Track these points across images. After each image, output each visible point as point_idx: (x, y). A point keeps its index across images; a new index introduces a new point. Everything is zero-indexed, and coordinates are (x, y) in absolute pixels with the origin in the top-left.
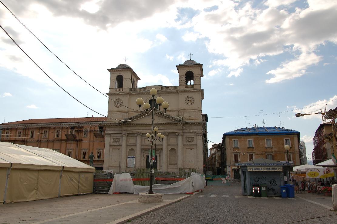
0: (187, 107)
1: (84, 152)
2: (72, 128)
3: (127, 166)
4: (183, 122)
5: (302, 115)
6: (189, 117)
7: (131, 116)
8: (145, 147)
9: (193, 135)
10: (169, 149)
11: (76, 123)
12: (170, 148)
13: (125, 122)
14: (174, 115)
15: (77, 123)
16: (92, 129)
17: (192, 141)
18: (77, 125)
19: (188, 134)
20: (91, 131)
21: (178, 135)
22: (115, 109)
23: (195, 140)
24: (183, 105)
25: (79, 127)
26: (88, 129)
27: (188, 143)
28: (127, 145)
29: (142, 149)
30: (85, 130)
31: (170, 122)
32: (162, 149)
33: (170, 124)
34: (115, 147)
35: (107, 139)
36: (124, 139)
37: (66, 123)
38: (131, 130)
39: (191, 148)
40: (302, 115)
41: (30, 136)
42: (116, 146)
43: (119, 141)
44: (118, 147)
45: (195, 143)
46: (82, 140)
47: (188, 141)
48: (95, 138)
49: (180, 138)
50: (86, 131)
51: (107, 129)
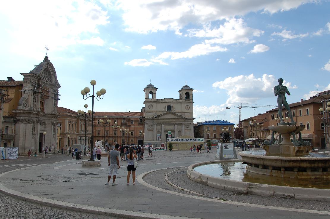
0: (186, 111)
2: (124, 119)
5: (229, 108)
6: (187, 115)
7: (159, 114)
8: (165, 130)
9: (189, 124)
10: (178, 131)
12: (178, 130)
13: (156, 117)
14: (180, 114)
16: (136, 120)
17: (189, 127)
19: (187, 124)
20: (135, 121)
21: (182, 125)
23: (190, 126)
24: (184, 110)
25: (127, 119)
27: (187, 128)
28: (157, 129)
29: (164, 131)
31: (179, 118)
32: (175, 131)
33: (179, 119)
34: (150, 130)
35: (146, 125)
36: (155, 125)
38: (159, 121)
40: (229, 108)
41: (98, 123)
42: (151, 130)
43: (152, 127)
44: (152, 130)
45: (190, 128)
46: (130, 126)
48: (138, 125)
49: (183, 126)
51: (146, 120)
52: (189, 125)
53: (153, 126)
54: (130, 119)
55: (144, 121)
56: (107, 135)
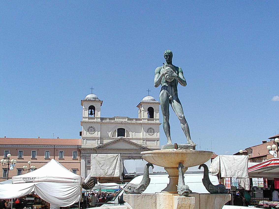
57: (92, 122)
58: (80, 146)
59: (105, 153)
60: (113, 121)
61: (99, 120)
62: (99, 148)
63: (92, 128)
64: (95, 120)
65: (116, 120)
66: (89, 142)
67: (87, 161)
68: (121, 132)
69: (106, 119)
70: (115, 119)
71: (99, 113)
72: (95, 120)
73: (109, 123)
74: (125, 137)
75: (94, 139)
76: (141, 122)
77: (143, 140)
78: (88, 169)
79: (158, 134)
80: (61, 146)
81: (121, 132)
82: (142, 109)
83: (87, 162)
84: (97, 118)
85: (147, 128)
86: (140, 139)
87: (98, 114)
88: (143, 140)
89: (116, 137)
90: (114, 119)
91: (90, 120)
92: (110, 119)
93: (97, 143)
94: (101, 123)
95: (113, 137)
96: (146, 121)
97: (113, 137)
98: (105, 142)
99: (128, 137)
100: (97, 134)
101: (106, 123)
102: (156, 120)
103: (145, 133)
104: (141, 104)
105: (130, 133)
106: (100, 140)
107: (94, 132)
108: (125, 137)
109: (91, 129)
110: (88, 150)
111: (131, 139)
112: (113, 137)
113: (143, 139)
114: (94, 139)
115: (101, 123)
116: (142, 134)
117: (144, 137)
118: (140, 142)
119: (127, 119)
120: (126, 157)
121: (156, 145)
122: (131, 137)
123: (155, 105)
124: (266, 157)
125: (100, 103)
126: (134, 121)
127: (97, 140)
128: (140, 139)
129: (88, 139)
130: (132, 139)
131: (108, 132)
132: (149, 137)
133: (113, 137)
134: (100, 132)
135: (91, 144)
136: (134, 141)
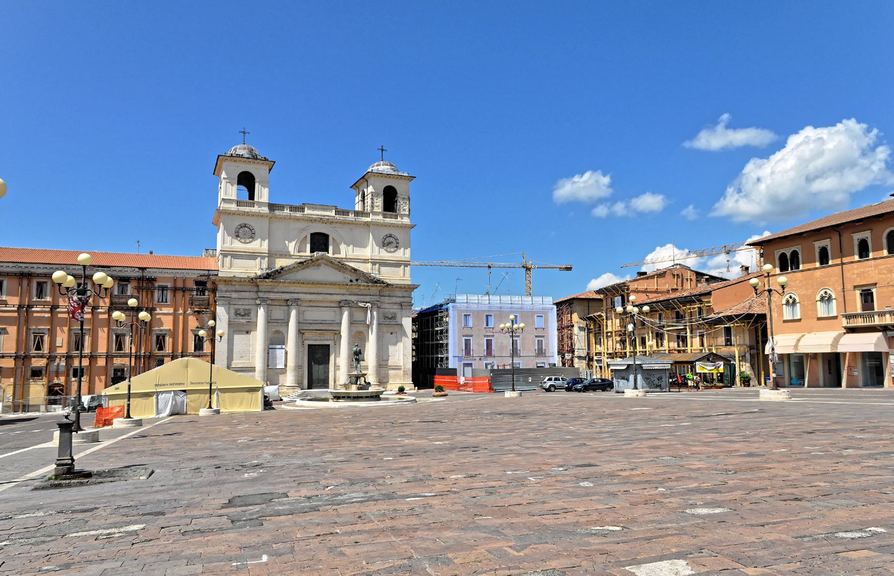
1: (158, 337)
3: (268, 366)
4: (384, 283)
9: (396, 307)
10: (353, 333)
11: (137, 270)
15: (140, 268)
16: (180, 284)
17: (394, 317)
18: (139, 274)
22: (238, 245)
23: (398, 316)
25: (140, 279)
26: (169, 285)
30: (159, 287)
37: (109, 267)
39: (392, 331)
47: (386, 317)
50: (163, 289)
52: (395, 309)
53: (253, 314)
54: (152, 280)
55: (214, 291)
56: (38, 348)
57: (247, 214)
58: (216, 273)
59: (280, 290)
60: (299, 214)
61: (265, 210)
62: (265, 278)
63: (246, 229)
64: (256, 209)
65: (307, 211)
66: (237, 262)
67: (233, 311)
68: (320, 242)
69: (281, 207)
70: (306, 209)
71: (266, 191)
72: (256, 209)
73: (290, 218)
74: (330, 254)
75: (252, 256)
76: (369, 219)
77: (371, 262)
78: (240, 332)
79: (408, 251)
80: (161, 270)
81: (320, 242)
82: (370, 189)
83: (233, 315)
84: (261, 204)
85: (383, 235)
86: (365, 261)
87: (263, 194)
88: (371, 262)
89: (308, 253)
90: (302, 209)
91: (242, 209)
92: (293, 208)
93: (258, 267)
94: (271, 219)
95: (301, 254)
96: (380, 218)
97: (298, 252)
98: (280, 263)
99: (336, 256)
100: (260, 245)
101: (284, 218)
102: (402, 216)
103: (377, 248)
104: (365, 177)
105: (343, 247)
106: (266, 259)
107: (251, 240)
108: (330, 254)
109: (244, 231)
110: (237, 284)
111: (342, 258)
112: (299, 252)
113: (371, 259)
114: (252, 256)
115: (271, 219)
116: (371, 250)
117: (374, 256)
118: (366, 268)
119: (334, 211)
120: (332, 302)
121: (402, 275)
122: (343, 255)
123: (400, 181)
124: (708, 296)
125: (267, 168)
126: (351, 217)
127: (259, 258)
128: (365, 261)
129: (236, 255)
130: (347, 259)
131: (287, 242)
132: (385, 255)
133: (301, 254)
134: (267, 241)
135: (243, 268)
136: (352, 265)
